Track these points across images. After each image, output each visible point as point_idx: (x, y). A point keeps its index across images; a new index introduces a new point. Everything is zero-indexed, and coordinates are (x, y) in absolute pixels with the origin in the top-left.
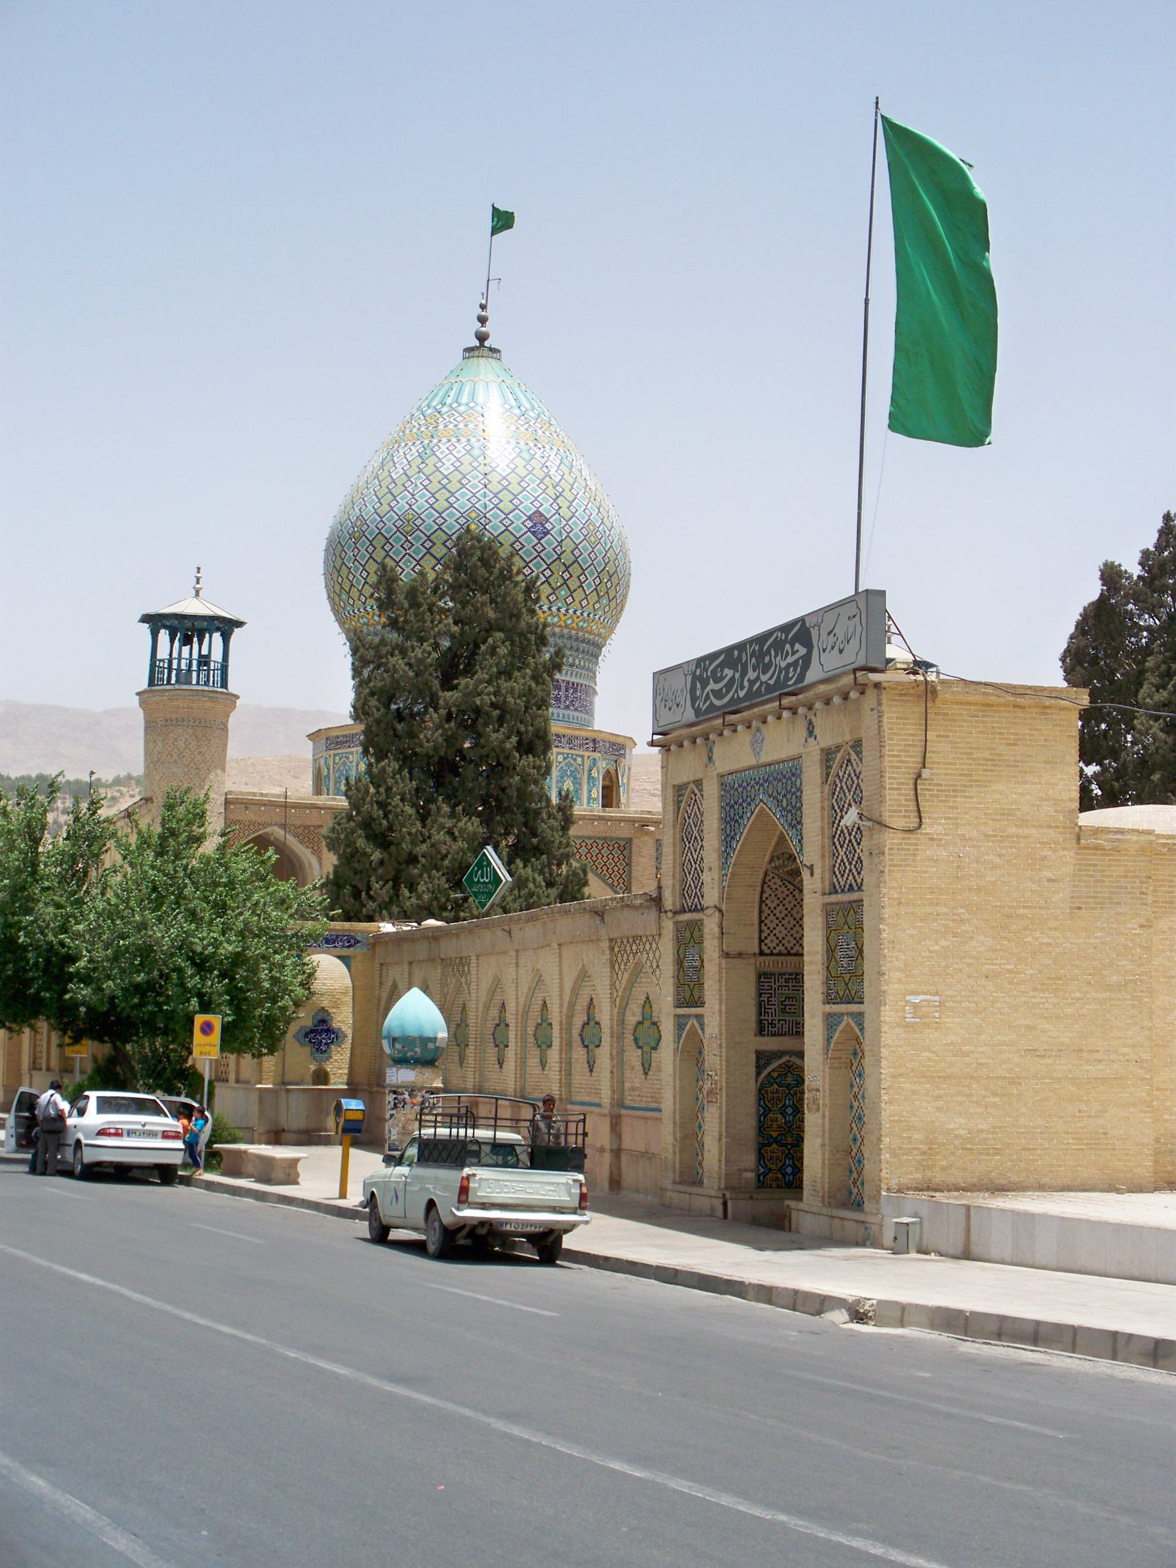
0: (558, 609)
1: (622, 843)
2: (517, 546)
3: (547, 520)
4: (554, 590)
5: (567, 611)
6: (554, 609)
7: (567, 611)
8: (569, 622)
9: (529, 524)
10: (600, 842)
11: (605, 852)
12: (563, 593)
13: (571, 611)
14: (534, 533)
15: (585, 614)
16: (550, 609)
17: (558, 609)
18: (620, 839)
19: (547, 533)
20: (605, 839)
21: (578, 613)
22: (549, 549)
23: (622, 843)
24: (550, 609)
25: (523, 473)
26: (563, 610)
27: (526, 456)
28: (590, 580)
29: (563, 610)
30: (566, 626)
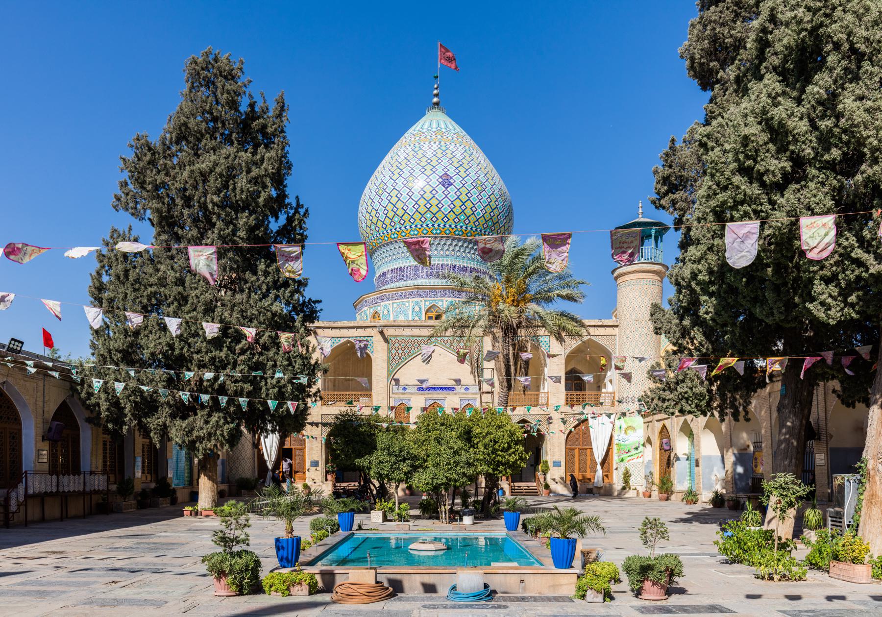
2: (434, 192)
3: (451, 178)
9: (440, 180)
14: (443, 185)
19: (452, 184)
22: (452, 193)
25: (439, 155)
26: (464, 228)
27: (444, 148)
28: (479, 210)
29: (464, 228)
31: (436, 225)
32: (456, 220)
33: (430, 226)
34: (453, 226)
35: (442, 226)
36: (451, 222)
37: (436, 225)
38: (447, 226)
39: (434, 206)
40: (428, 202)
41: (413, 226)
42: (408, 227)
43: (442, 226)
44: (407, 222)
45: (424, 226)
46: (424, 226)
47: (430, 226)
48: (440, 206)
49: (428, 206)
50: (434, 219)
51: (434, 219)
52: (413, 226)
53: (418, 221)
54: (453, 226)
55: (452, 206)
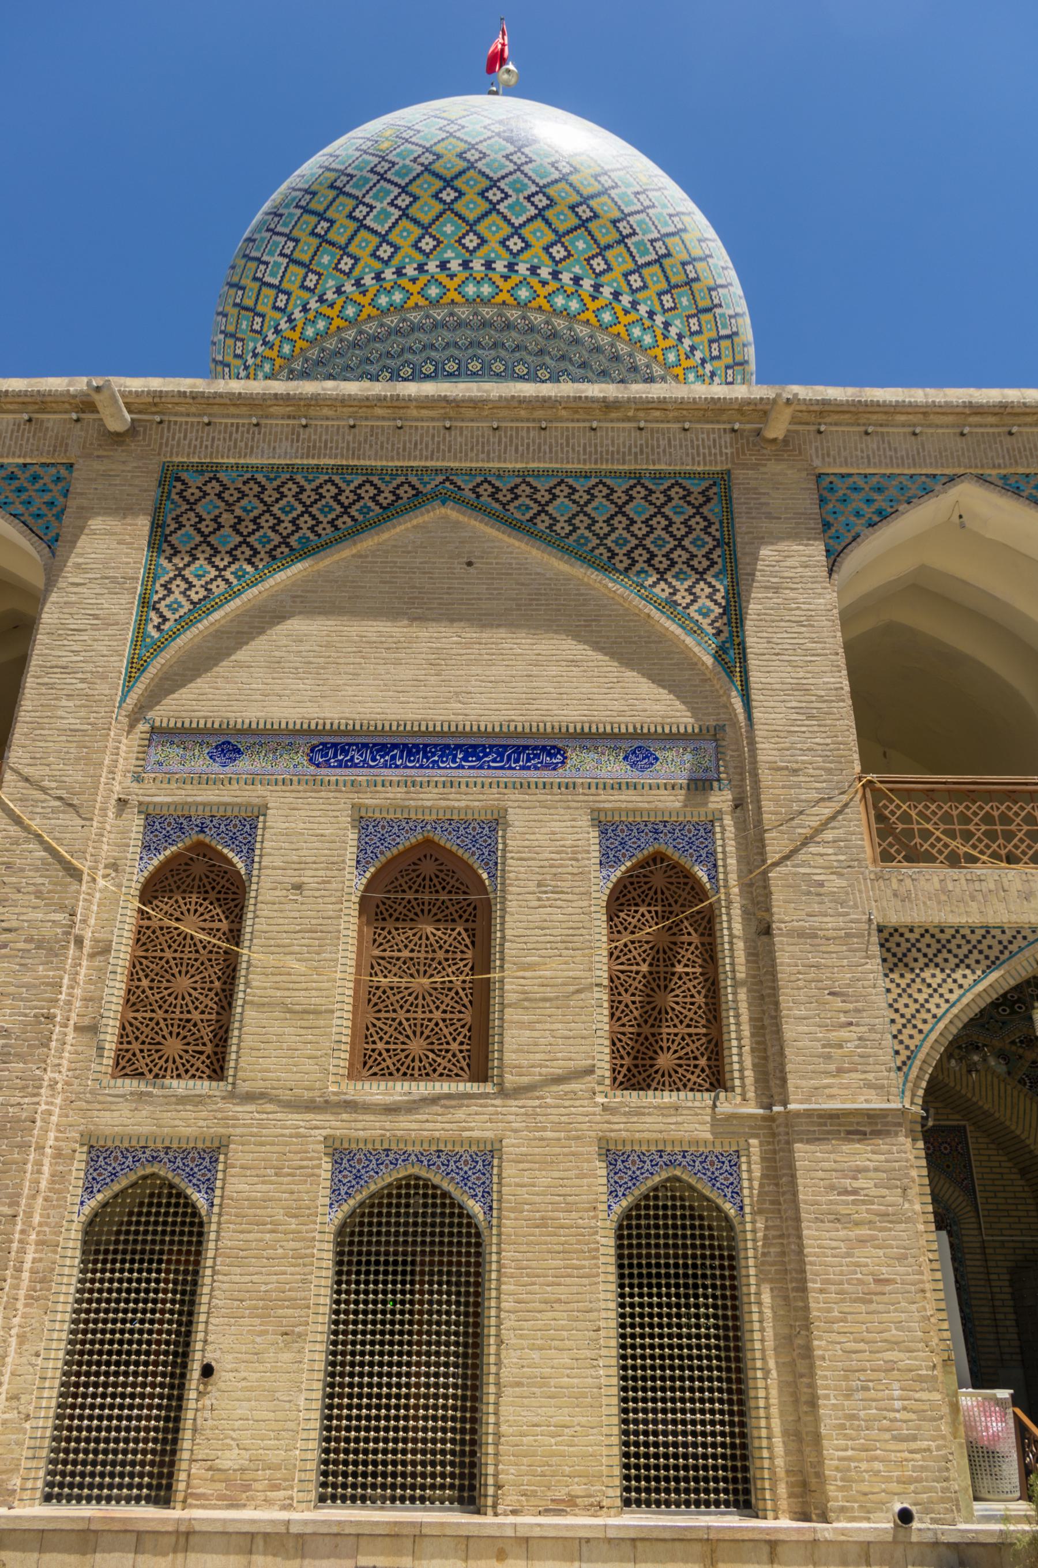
0: (577, 280)
1: (696, 487)
4: (560, 237)
5: (597, 287)
6: (566, 277)
7: (597, 287)
8: (607, 317)
10: (621, 486)
11: (638, 509)
12: (581, 245)
13: (607, 291)
15: (643, 309)
16: (555, 275)
17: (577, 280)
18: (689, 475)
20: (637, 478)
21: (626, 299)
23: (696, 487)
24: (555, 275)
26: (587, 284)
29: (587, 284)
30: (604, 328)
31: (477, 265)
32: (558, 252)
33: (454, 266)
34: (545, 273)
35: (500, 266)
36: (536, 254)
37: (477, 265)
38: (522, 268)
39: (471, 195)
40: (449, 207)
41: (389, 274)
42: (368, 280)
43: (500, 266)
44: (366, 259)
45: (432, 267)
46: (432, 267)
47: (454, 266)
48: (494, 195)
49: (448, 195)
50: (471, 241)
51: (471, 241)
52: (389, 274)
53: (407, 249)
54: (545, 273)
55: (541, 201)
